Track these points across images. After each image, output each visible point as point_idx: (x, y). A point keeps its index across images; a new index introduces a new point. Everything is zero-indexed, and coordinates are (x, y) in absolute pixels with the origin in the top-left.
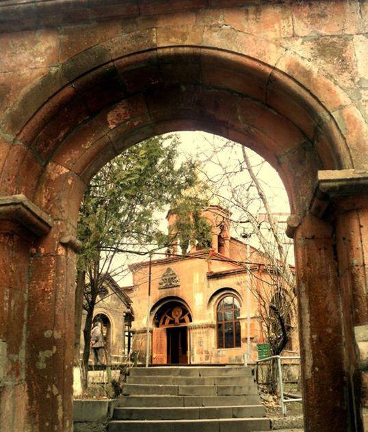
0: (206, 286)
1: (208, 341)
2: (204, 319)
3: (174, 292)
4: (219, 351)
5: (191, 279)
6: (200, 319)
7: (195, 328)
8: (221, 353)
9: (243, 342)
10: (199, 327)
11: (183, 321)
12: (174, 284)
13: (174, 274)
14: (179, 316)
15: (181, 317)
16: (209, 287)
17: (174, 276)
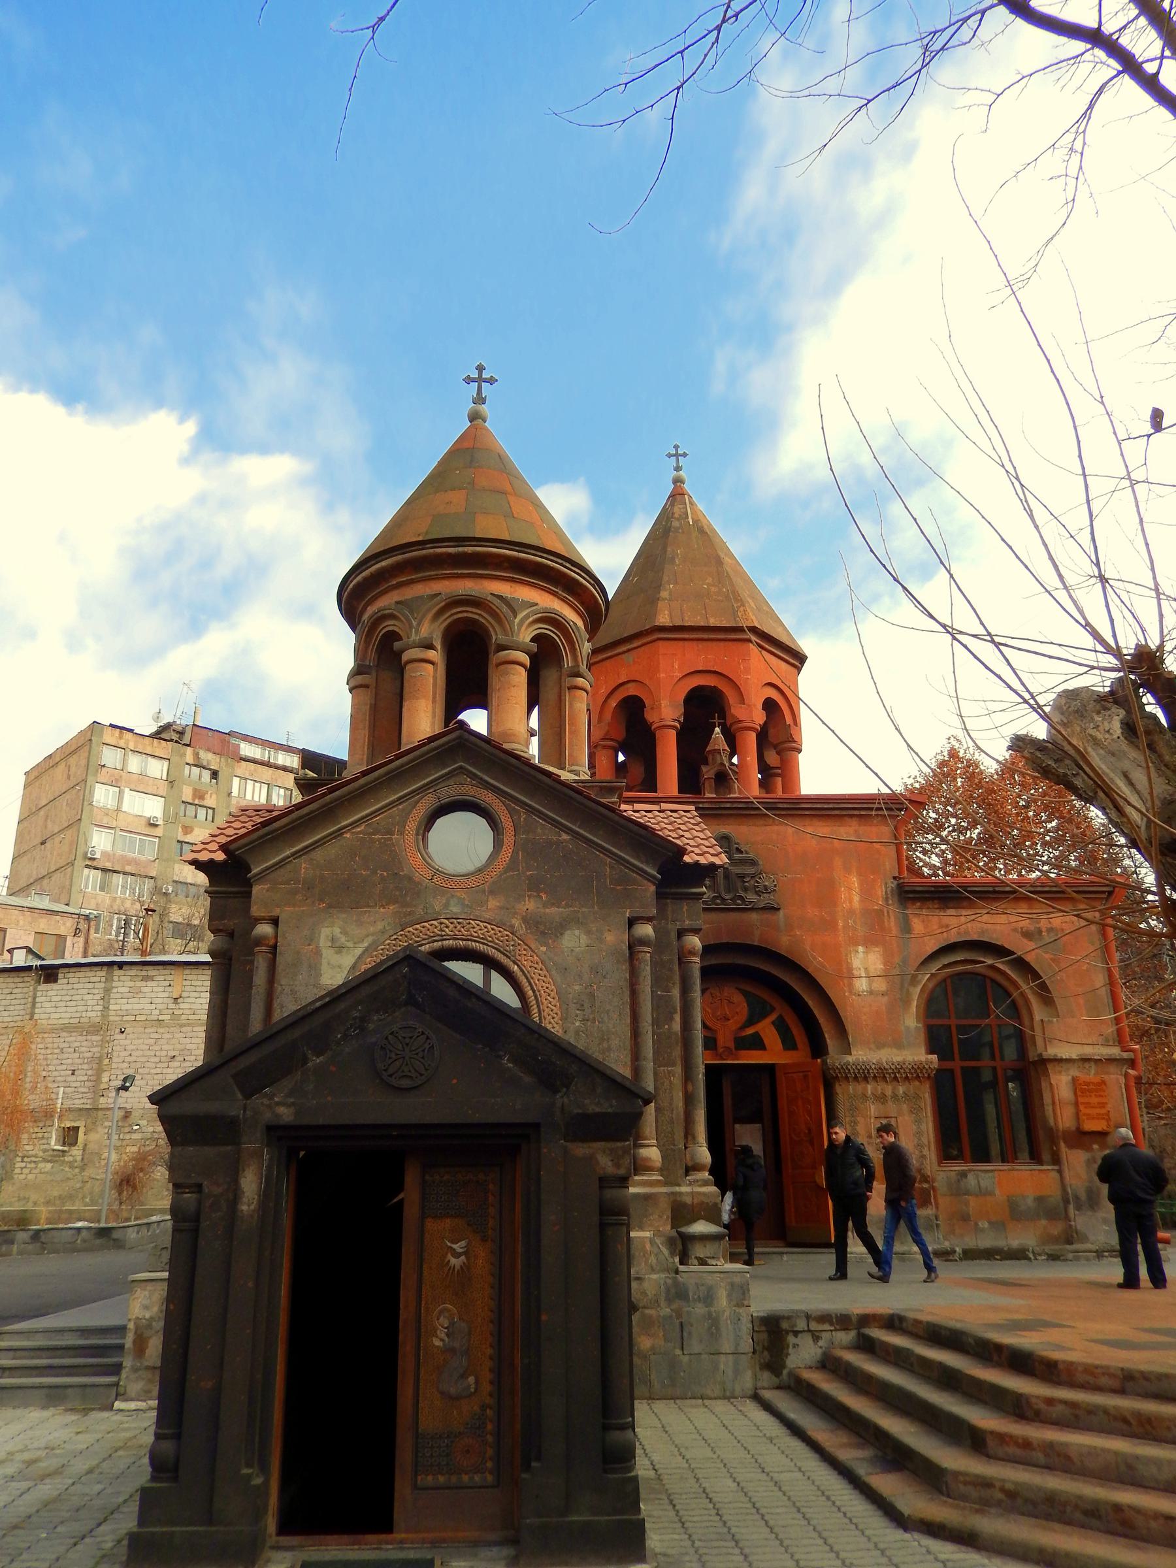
0: (892, 924)
1: (919, 1133)
2: (898, 1045)
3: (755, 927)
4: (963, 1175)
5: (827, 896)
6: (880, 1046)
7: (864, 1075)
8: (971, 1180)
9: (1071, 1146)
10: (882, 1074)
11: (757, 1043)
12: (751, 897)
13: (753, 863)
14: (733, 1024)
15: (743, 1028)
16: (906, 928)
17: (750, 870)
